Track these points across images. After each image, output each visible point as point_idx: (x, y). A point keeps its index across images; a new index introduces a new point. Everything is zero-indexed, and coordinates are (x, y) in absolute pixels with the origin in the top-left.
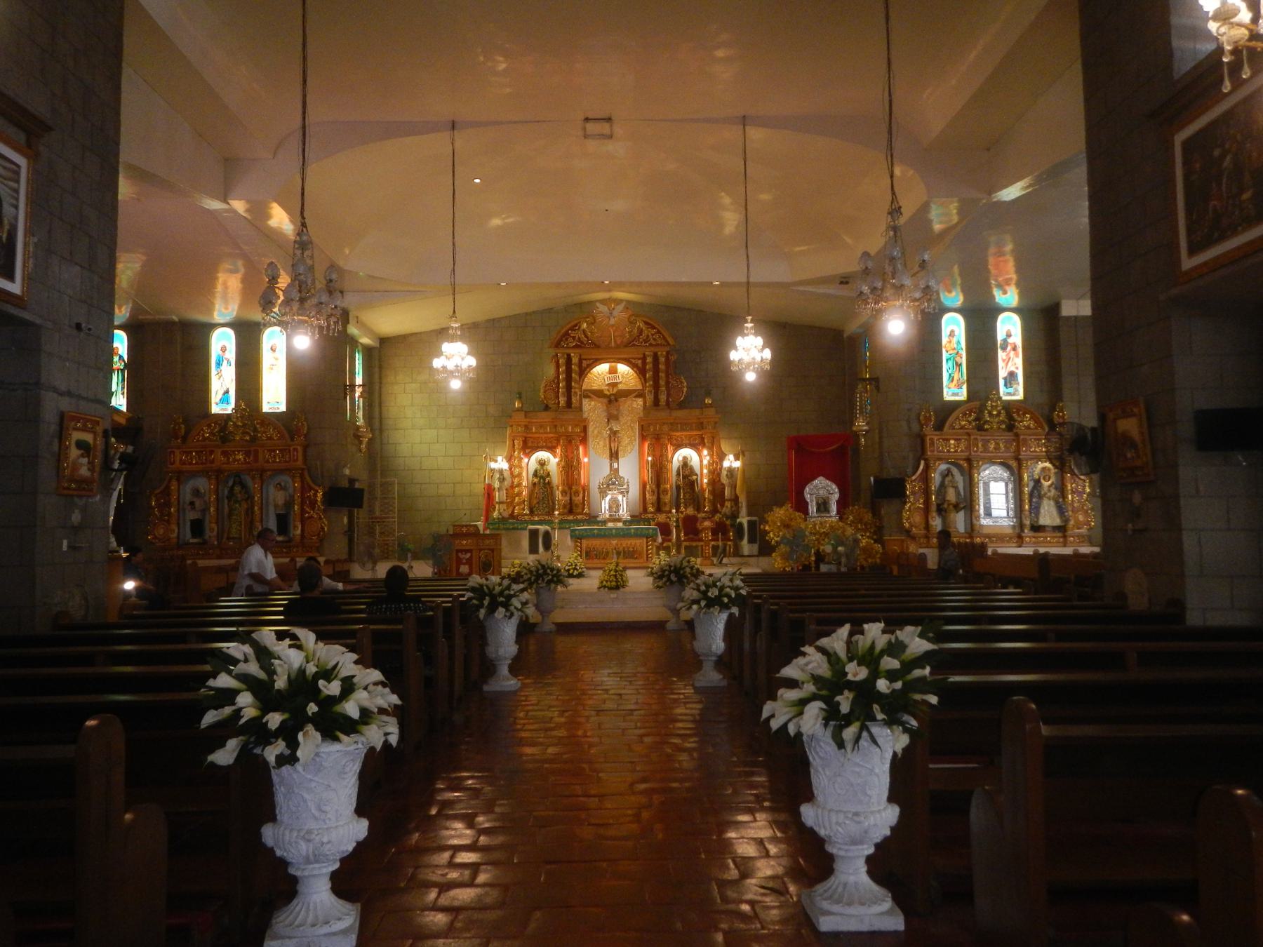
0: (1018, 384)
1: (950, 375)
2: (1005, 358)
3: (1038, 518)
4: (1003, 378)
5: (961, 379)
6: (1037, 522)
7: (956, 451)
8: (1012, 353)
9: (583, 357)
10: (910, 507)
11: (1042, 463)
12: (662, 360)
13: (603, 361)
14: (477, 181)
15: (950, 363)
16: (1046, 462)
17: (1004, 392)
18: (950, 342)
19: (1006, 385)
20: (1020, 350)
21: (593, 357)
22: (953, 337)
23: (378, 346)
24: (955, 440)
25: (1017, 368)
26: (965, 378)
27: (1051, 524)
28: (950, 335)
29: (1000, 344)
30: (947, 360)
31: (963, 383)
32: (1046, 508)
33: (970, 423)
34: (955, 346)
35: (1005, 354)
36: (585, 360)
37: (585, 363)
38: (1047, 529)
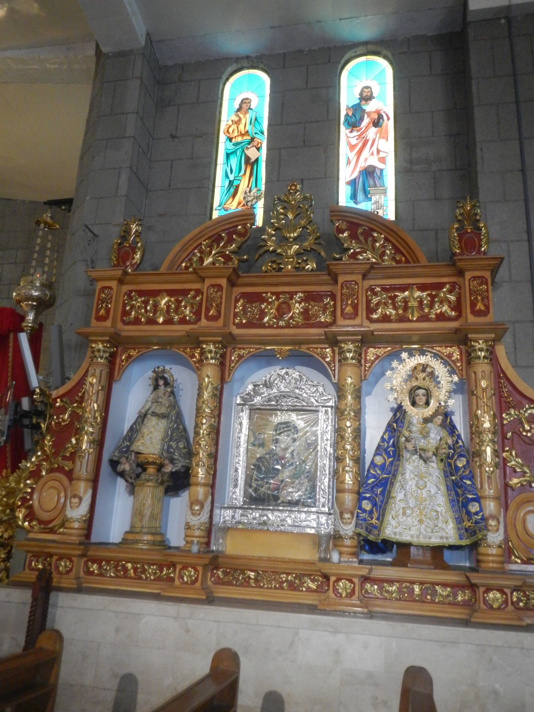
0: (384, 192)
1: (231, 183)
2: (354, 141)
3: (381, 518)
4: (348, 183)
5: (254, 190)
6: (379, 528)
7: (168, 321)
8: (373, 131)
10: (39, 467)
11: (411, 355)
15: (234, 161)
16: (452, 372)
18: (238, 123)
20: (390, 125)
22: (246, 112)
24: (170, 293)
25: (383, 160)
26: (263, 188)
27: (423, 541)
28: (239, 110)
29: (347, 115)
30: (228, 156)
31: (258, 198)
32: (411, 485)
33: (228, 259)
34: (248, 127)
35: (355, 133)
38: (413, 549)
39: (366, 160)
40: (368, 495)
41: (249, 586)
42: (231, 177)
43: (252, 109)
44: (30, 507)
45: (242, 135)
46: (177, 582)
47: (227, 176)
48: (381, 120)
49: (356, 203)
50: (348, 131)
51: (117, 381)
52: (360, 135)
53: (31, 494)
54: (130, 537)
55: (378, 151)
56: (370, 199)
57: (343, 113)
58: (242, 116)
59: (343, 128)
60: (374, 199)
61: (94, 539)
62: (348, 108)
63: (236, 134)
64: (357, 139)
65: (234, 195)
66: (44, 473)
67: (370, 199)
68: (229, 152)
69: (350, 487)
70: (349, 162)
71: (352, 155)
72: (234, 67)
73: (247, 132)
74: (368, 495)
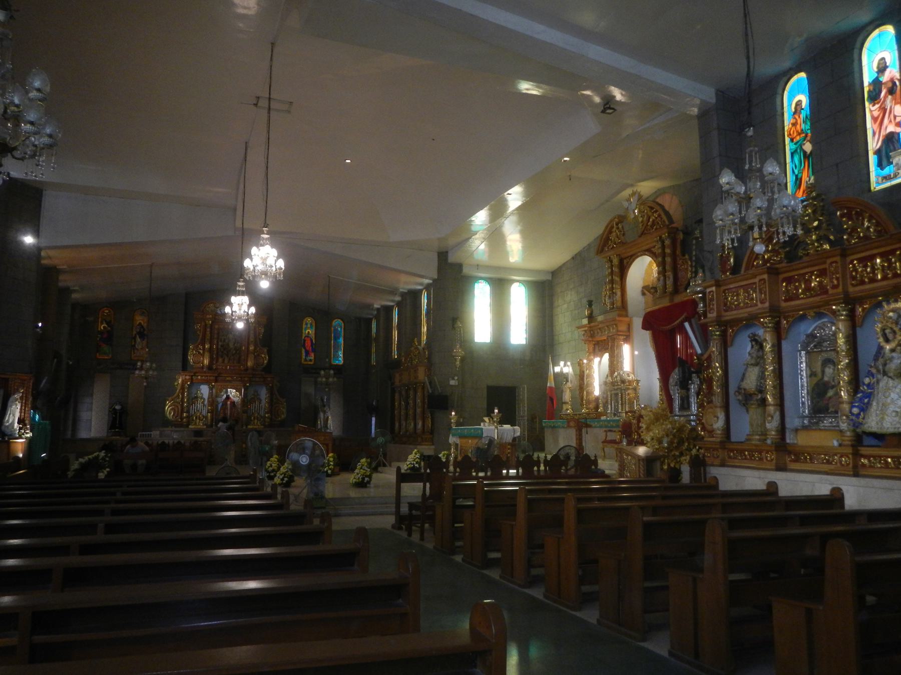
1: (797, 176)
2: (876, 114)
9: (623, 256)
12: (667, 242)
13: (634, 257)
14: (348, 161)
15: (796, 158)
17: (877, 176)
18: (794, 125)
19: (880, 165)
21: (629, 254)
23: (550, 278)
28: (795, 113)
29: (869, 92)
30: (792, 154)
35: (877, 106)
36: (625, 258)
37: (625, 261)
39: (886, 128)
40: (857, 404)
41: (807, 462)
42: (796, 172)
43: (803, 109)
44: (703, 424)
45: (799, 134)
46: (765, 460)
47: (793, 172)
48: (895, 87)
49: (882, 169)
50: (871, 105)
51: (732, 345)
52: (880, 107)
53: (702, 417)
54: (750, 437)
55: (895, 117)
56: (892, 163)
57: (866, 90)
58: (797, 117)
59: (867, 104)
60: (894, 163)
61: (733, 439)
62: (870, 84)
63: (795, 134)
64: (879, 111)
65: (799, 187)
66: (705, 404)
67: (892, 163)
68: (792, 151)
69: (847, 400)
70: (874, 134)
71: (876, 127)
72: (785, 79)
73: (802, 130)
74: (857, 404)
